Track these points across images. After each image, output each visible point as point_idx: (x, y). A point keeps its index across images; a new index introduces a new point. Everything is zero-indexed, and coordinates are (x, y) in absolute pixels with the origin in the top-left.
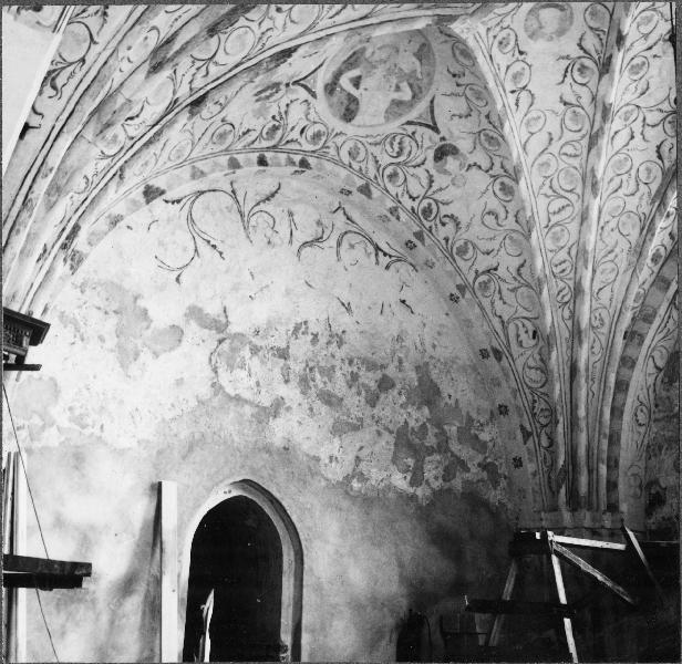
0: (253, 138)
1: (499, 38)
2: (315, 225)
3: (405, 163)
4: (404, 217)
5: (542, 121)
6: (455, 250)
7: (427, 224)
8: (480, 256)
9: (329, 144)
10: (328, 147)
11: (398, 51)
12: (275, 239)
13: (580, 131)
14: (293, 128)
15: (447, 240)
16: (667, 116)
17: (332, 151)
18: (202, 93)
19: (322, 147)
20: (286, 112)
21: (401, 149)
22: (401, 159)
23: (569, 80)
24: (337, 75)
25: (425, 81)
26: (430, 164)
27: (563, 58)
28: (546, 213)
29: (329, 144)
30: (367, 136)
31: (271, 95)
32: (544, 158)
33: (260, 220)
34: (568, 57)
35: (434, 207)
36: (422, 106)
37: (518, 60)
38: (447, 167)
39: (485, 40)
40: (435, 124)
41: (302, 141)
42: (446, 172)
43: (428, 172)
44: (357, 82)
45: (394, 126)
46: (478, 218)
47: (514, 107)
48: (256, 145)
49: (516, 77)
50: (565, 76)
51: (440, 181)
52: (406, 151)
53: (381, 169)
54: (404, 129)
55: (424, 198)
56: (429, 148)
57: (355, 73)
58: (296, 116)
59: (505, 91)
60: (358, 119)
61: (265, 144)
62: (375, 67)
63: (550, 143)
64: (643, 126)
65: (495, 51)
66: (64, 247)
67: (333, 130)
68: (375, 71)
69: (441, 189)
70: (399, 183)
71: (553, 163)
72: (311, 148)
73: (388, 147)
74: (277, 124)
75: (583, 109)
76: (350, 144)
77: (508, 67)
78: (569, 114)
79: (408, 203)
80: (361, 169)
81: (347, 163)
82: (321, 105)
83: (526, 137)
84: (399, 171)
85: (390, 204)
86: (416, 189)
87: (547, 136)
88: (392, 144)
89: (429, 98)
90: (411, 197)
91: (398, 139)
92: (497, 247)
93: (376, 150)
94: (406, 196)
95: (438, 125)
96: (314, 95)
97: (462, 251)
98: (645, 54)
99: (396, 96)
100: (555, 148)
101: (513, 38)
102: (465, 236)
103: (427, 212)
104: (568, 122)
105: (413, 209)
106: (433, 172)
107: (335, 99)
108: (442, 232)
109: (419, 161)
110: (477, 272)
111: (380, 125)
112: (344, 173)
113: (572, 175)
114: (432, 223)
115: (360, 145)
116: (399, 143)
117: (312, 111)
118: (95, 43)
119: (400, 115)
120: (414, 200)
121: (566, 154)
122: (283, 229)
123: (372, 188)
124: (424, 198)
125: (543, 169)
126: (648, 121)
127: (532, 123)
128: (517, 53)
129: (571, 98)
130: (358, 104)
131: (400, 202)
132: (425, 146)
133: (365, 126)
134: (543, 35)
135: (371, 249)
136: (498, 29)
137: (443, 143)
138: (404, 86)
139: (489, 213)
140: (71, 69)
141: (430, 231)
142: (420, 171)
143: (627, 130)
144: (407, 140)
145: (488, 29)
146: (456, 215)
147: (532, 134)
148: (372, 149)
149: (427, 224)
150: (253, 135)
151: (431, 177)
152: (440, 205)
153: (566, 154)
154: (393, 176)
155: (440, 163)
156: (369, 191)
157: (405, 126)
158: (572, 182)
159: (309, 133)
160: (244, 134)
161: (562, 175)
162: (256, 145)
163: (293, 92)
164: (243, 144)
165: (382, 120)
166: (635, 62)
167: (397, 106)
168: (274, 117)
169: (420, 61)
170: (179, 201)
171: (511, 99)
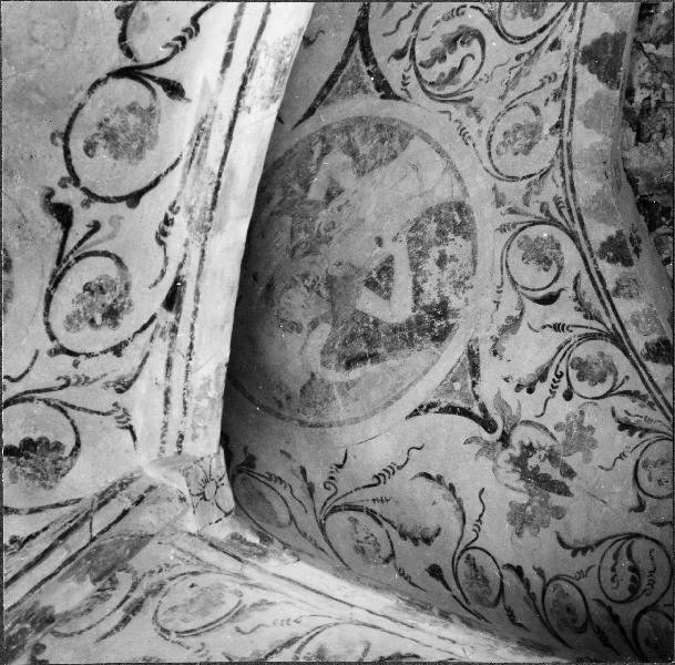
1: (110, 336)
9: (535, 210)
14: (557, 327)
19: (552, 222)
20: (542, 377)
21: (452, 42)
29: (535, 210)
37: (92, 197)
39: (156, 365)
40: (352, 42)
41: (566, 282)
48: (635, 384)
52: (451, 27)
57: (368, 303)
58: (531, 350)
60: (444, 191)
61: (623, 365)
62: (330, 281)
65: (146, 301)
67: (503, 229)
72: (570, 253)
73: (465, 75)
74: (573, 373)
76: (509, 162)
77: (134, 199)
82: (476, 318)
88: (455, 72)
95: (346, 36)
96: (472, 355)
101: (65, 301)
111: (426, 138)
115: (498, 138)
128: (79, 228)
133: (451, 167)
144: (422, 52)
145: (123, 386)
148: (490, 108)
156: (597, 43)
162: (635, 384)
163: (502, 405)
164: (647, 411)
165: (416, 144)
168: (568, 396)
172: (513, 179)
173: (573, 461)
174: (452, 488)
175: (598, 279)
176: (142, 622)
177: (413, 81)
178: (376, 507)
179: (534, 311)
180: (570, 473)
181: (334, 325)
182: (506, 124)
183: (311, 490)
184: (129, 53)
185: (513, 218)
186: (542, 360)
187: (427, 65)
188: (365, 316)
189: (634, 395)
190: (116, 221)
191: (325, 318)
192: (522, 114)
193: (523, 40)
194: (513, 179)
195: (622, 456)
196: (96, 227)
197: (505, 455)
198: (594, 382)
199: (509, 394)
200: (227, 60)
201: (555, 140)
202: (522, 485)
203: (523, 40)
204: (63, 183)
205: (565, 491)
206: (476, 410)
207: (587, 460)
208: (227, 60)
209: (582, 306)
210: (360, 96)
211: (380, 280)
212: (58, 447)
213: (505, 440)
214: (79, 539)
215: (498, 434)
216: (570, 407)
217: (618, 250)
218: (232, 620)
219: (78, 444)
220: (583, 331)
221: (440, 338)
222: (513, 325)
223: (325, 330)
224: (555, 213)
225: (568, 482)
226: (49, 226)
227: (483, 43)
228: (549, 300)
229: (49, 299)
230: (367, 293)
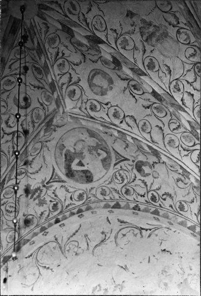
1: (88, 108)
2: (101, 234)
4: (142, 207)
5: (147, 122)
6: (178, 210)
7: (157, 204)
8: (190, 204)
10: (90, 197)
11: (83, 141)
12: (80, 251)
13: (167, 114)
14: (65, 200)
15: (171, 206)
16: (194, 70)
17: (93, 199)
21: (122, 177)
22: (125, 182)
23: (137, 97)
24: (68, 167)
25: (104, 143)
26: (139, 176)
27: (124, 91)
28: (194, 165)
30: (105, 182)
32: (167, 140)
33: (71, 246)
34: (125, 89)
35: (155, 194)
36: (113, 155)
37: (109, 108)
38: (146, 172)
41: (74, 202)
42: (148, 175)
43: (140, 179)
44: (81, 164)
45: (111, 171)
46: (175, 186)
47: (129, 129)
48: (51, 216)
49: (116, 115)
50: (134, 97)
51: (149, 180)
52: (125, 177)
53: (120, 192)
54: (116, 169)
55: (148, 193)
56: (132, 169)
58: (61, 193)
59: (117, 127)
61: (56, 213)
62: (82, 153)
63: (163, 130)
64: (191, 85)
65: (92, 114)
67: (87, 189)
68: (84, 154)
69: (152, 184)
70: (132, 194)
71: (173, 138)
72: (81, 202)
73: (116, 180)
74: (55, 203)
75: (156, 103)
76: (100, 190)
77: (107, 114)
78: (155, 111)
80: (111, 198)
81: (103, 199)
82: (71, 183)
83: (149, 136)
84: (128, 188)
87: (158, 128)
89: (111, 149)
90: (141, 196)
91: (117, 174)
92: (194, 196)
93: (112, 185)
94: (139, 197)
96: (63, 181)
97: (182, 208)
98: (146, 55)
99: (101, 158)
100: (166, 130)
102: (177, 200)
103: (154, 198)
104: (159, 115)
105: (146, 201)
106: (143, 178)
107: (77, 177)
109: (133, 178)
110: (195, 214)
113: (188, 136)
114: (159, 202)
115: (104, 188)
116: (120, 176)
117: (69, 188)
119: (110, 164)
120: (144, 197)
121: (174, 129)
122: (83, 245)
123: (120, 203)
124: (148, 193)
125: (172, 144)
126: (190, 81)
127: (144, 128)
128: (104, 106)
129: (147, 103)
130: (90, 172)
131: (138, 201)
132: (130, 169)
134: (106, 90)
135: (137, 231)
136: (84, 104)
137: (135, 163)
138: (100, 151)
139: (178, 181)
141: (161, 207)
142: (137, 182)
143: (186, 96)
144: (121, 172)
145: (80, 109)
146: (167, 192)
147: (150, 133)
148: (109, 186)
151: (143, 181)
152: (157, 191)
153: (174, 129)
154: (127, 192)
155: (142, 172)
157: (116, 167)
158: (191, 141)
159: (76, 196)
161: (183, 140)
163: (51, 186)
164: (44, 218)
165: (106, 171)
166: (146, 63)
167: (105, 162)
168: (51, 201)
169: (95, 137)
170: (31, 255)
171: (124, 126)
172: (96, 191)
173: (37, 201)
174: (37, 172)
175: (74, 208)
176: (38, 105)
177: (116, 170)
178: (39, 154)
179: (69, 195)
180: (34, 200)
181: (74, 153)
183: (46, 142)
184: (127, 116)
185: (88, 191)
186: (59, 196)
187: (119, 173)
188: (74, 160)
189: (48, 216)
190: (105, 111)
191: (75, 151)
192: (108, 192)
193: (121, 191)
194: (96, 191)
195: (36, 212)
196: (104, 108)
197: (41, 185)
198: (53, 207)
199: (54, 188)
200: (125, 130)
201: (103, 199)
202: (34, 188)
203: (121, 191)
204: (111, 105)
205: (31, 198)
206: (51, 181)
207: (37, 204)
208: (125, 130)
209: (69, 205)
210: (115, 159)
211: (81, 164)
212: (73, 97)
213: (44, 186)
214: (61, 97)
215: (46, 185)
216: (48, 202)
218: (32, 121)
219: (73, 100)
220: (64, 204)
221: (67, 175)
222: (67, 191)
223: (73, 151)
224: (89, 199)
225: (33, 199)
226: (106, 101)
227: (121, 183)
228: (71, 198)
229: (95, 100)
230: (79, 161)
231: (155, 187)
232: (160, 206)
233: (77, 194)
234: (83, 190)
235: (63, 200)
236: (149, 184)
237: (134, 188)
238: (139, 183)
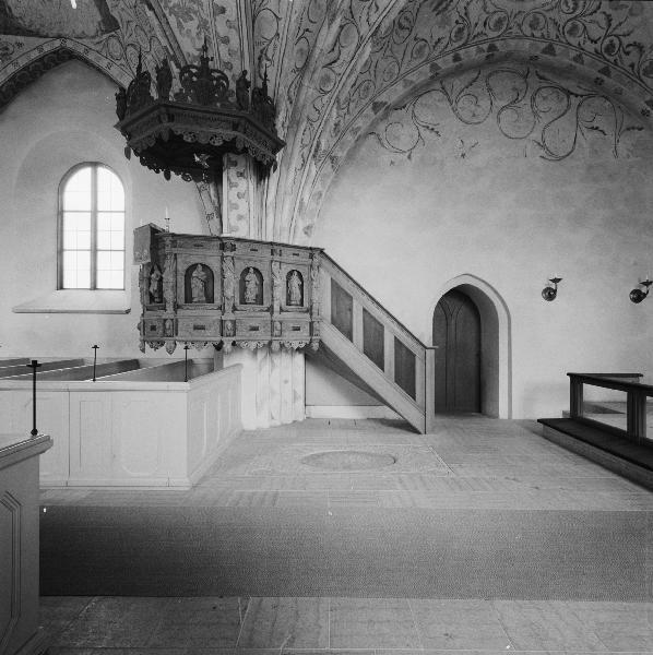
0: (445, 44)
3: (582, 15)
4: (586, 59)
6: (641, 72)
7: (612, 59)
14: (476, 24)
17: (515, 30)
18: (377, 23)
20: (466, 14)
22: (578, 12)
31: (448, 5)
35: (616, 42)
41: (487, 31)
43: (604, 13)
48: (450, 48)
51: (617, 17)
53: (561, 29)
66: (314, 156)
72: (496, 34)
73: (564, 8)
74: (461, 26)
76: (530, 18)
79: (590, 47)
80: (543, 35)
85: (573, 54)
86: (596, 32)
93: (551, 14)
94: (589, 43)
103: (610, 48)
105: (596, 51)
108: (627, 60)
109: (594, 7)
112: (527, 44)
115: (538, 15)
118: (280, 19)
135: (562, 95)
140: (272, 44)
142: (599, 17)
146: (638, 41)
149: (612, 59)
150: (445, 42)
151: (609, 16)
154: (573, 31)
160: (436, 43)
168: (457, 22)
175: (484, 41)
182: (541, 18)
207: (437, 23)
217: (492, 48)
231: (624, 29)
232: (616, 63)
233: (496, 17)
234: (506, 12)
235: (473, 22)
236: (614, 24)
237: (588, 26)
238: (599, 17)
